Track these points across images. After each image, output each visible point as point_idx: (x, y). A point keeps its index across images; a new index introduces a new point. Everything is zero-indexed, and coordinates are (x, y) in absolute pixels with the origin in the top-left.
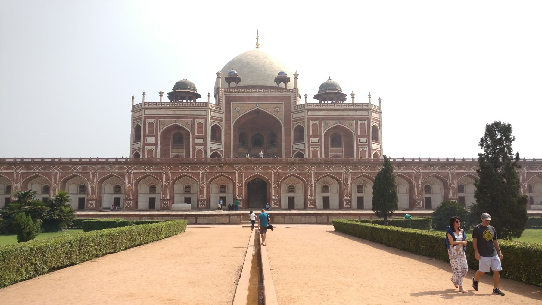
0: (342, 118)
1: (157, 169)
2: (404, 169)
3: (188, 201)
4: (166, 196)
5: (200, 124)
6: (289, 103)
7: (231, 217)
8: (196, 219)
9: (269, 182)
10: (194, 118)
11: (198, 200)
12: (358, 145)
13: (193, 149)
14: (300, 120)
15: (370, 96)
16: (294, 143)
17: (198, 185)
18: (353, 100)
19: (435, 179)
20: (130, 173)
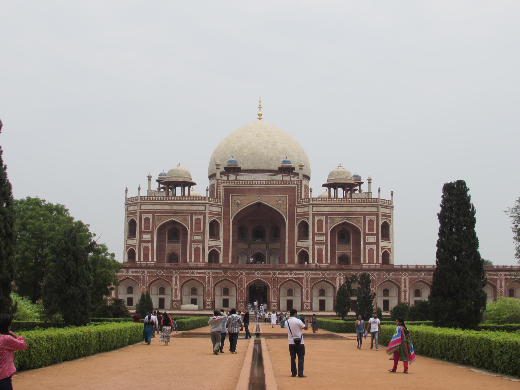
0: (350, 215)
1: (168, 273)
2: (393, 275)
3: (194, 302)
4: (176, 297)
5: (198, 220)
6: (294, 196)
9: (269, 287)
10: (192, 214)
12: (365, 244)
13: (191, 246)
15: (379, 191)
16: (298, 239)
18: (370, 188)
19: (424, 284)
20: (144, 277)
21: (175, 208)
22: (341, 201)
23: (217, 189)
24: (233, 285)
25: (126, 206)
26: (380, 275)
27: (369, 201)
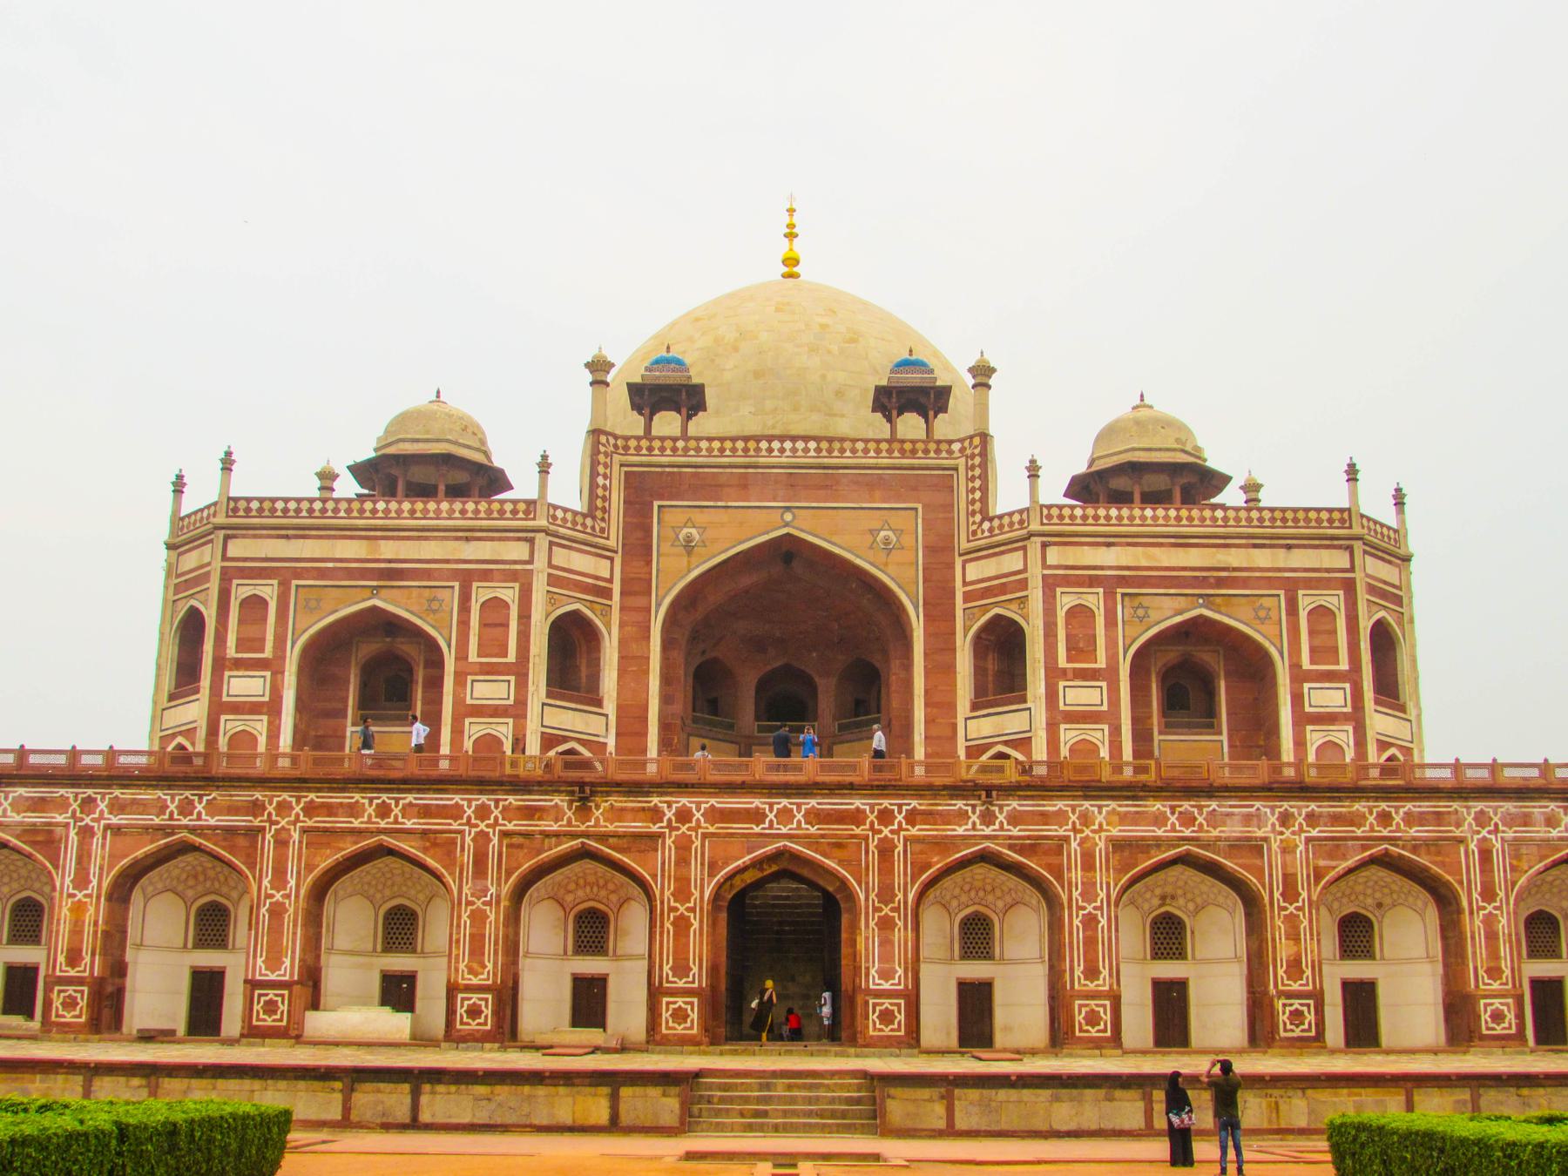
0: (1220, 583)
1: (233, 810)
3: (398, 992)
4: (274, 962)
5: (496, 605)
6: (949, 507)
7: (625, 1092)
8: (416, 1095)
9: (851, 897)
10: (467, 579)
11: (452, 990)
12: (1302, 719)
13: (458, 732)
14: (1003, 589)
15: (1352, 473)
17: (455, 906)
20: (86, 833)
21: (388, 550)
22: (1178, 519)
23: (594, 474)
24: (636, 890)
25: (174, 554)
26: (1526, 820)
27: (1307, 520)
